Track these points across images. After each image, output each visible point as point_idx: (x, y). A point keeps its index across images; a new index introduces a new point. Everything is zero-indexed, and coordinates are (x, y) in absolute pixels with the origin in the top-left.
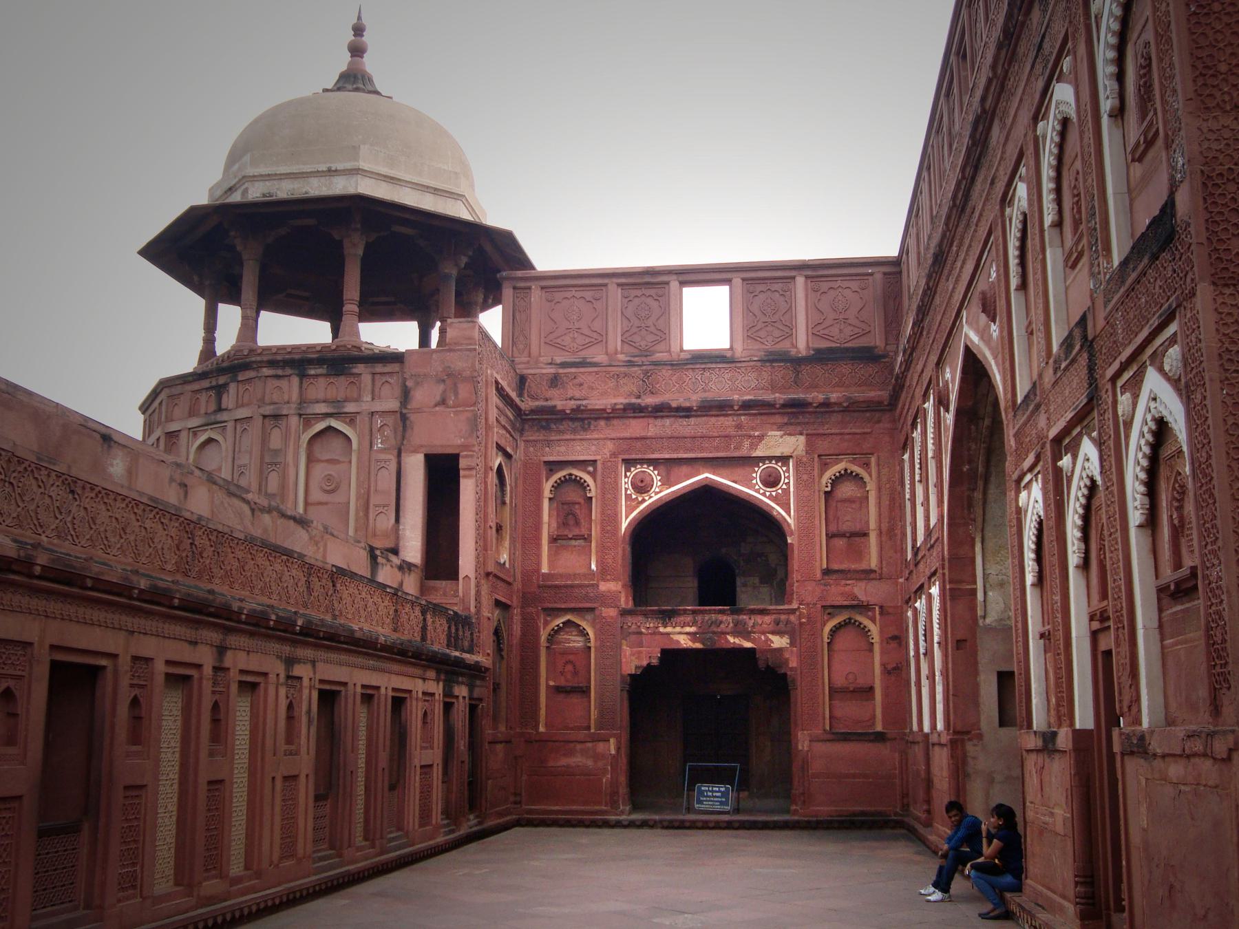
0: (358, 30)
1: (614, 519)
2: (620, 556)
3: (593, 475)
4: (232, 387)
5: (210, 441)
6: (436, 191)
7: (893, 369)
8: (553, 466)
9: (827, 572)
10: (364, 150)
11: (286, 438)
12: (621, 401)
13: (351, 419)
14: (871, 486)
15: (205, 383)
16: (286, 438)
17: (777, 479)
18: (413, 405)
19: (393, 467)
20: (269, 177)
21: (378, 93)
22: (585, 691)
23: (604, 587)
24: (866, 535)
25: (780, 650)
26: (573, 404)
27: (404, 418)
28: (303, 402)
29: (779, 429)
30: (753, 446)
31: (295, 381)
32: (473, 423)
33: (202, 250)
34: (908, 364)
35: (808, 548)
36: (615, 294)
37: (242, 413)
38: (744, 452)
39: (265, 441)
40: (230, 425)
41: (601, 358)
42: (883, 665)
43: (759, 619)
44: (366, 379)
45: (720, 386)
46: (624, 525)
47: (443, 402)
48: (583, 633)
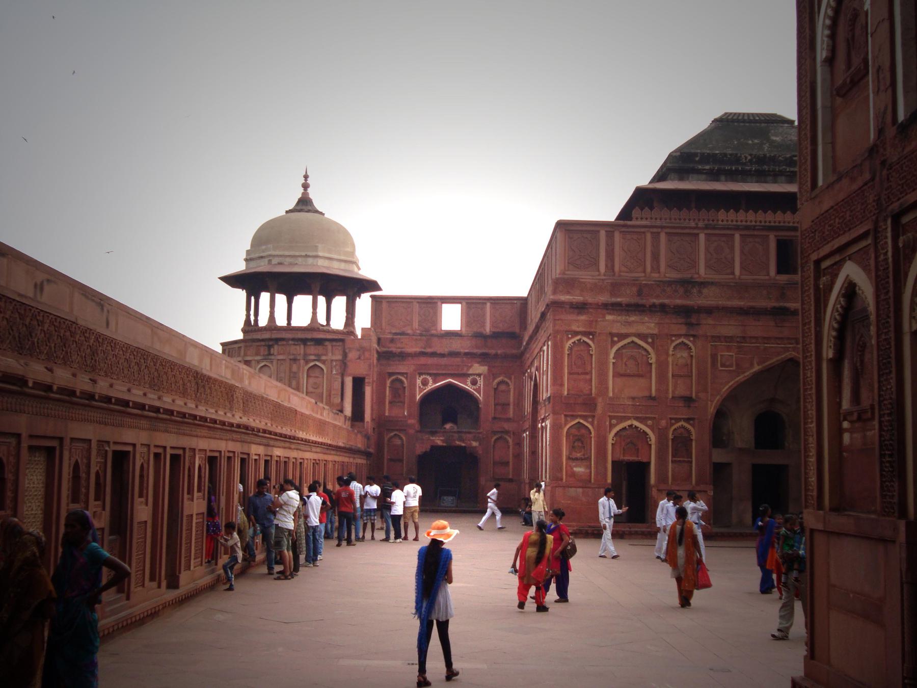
0: (306, 177)
1: (415, 396)
2: (416, 410)
3: (406, 378)
4: (276, 347)
5: (265, 365)
6: (345, 261)
7: (522, 343)
8: (391, 374)
9: (494, 418)
10: (320, 246)
11: (299, 368)
12: (418, 350)
13: (324, 362)
14: (512, 387)
15: (263, 343)
16: (299, 368)
17: (476, 382)
18: (348, 359)
19: (340, 380)
20: (281, 256)
21: (317, 211)
22: (401, 461)
23: (410, 421)
24: (509, 405)
25: (476, 447)
26: (399, 350)
27: (345, 364)
28: (305, 355)
29: (478, 363)
30: (468, 370)
31: (302, 346)
32: (370, 365)
33: (251, 282)
34: (526, 349)
35: (487, 409)
36: (416, 306)
37: (281, 357)
38: (464, 371)
39: (290, 369)
40: (275, 362)
41: (409, 332)
42: (513, 454)
43: (468, 435)
44: (330, 347)
45: (456, 345)
46: (418, 397)
47: (359, 358)
48: (401, 439)
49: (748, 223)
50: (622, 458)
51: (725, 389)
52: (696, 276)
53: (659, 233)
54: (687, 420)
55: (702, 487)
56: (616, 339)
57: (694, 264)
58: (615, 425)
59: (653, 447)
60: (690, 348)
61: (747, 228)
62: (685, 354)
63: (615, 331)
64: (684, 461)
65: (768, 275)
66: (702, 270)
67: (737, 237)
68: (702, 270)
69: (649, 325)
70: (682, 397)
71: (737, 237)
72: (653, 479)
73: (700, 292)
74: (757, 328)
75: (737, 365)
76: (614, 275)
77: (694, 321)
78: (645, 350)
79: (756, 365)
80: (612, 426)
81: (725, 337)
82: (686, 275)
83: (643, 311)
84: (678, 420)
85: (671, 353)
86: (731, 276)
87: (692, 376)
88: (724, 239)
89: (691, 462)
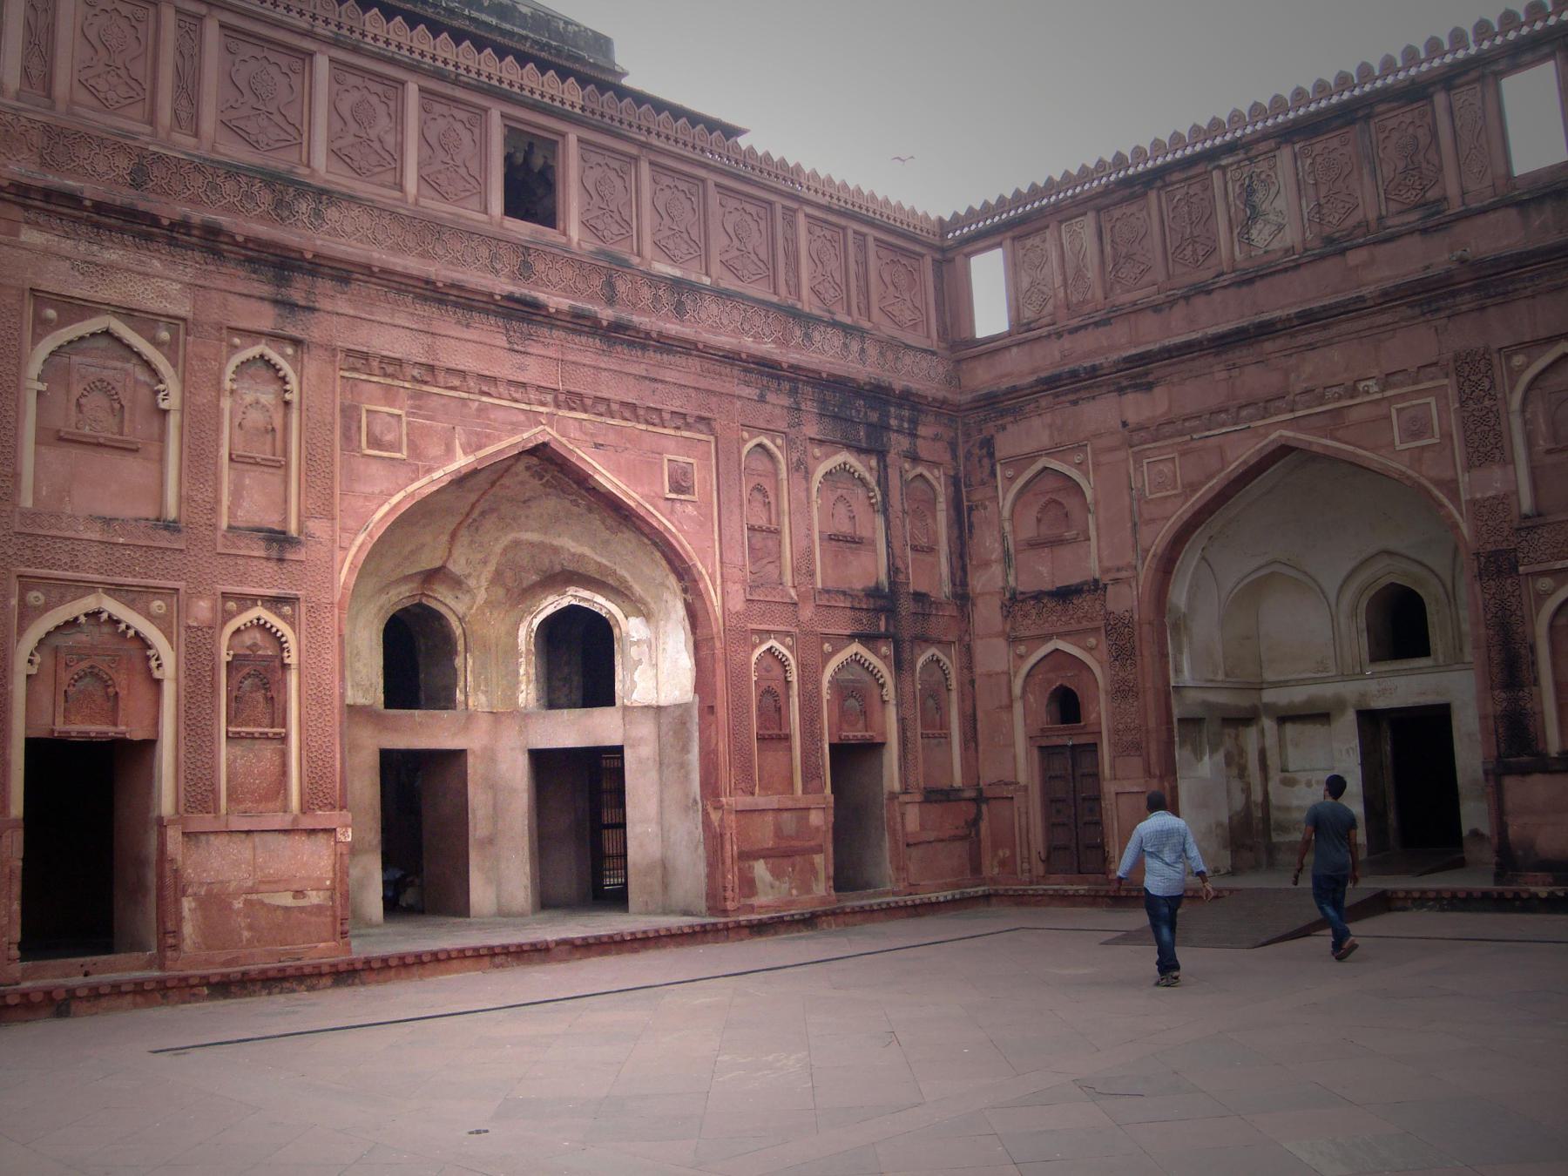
49: (439, 64)
50: (60, 727)
51: (381, 514)
52: (303, 171)
53: (200, 18)
54: (275, 602)
55: (322, 818)
56: (51, 313)
57: (297, 136)
58: (47, 608)
59: (169, 690)
60: (284, 380)
61: (439, 75)
62: (268, 396)
63: (49, 284)
64: (265, 737)
65: (486, 212)
66: (320, 159)
67: (412, 89)
68: (320, 159)
69: (164, 284)
70: (259, 530)
71: (412, 89)
72: (166, 800)
73: (318, 214)
74: (470, 346)
75: (413, 447)
76: (52, 107)
77: (298, 296)
78: (148, 365)
79: (459, 451)
80: (27, 614)
81: (384, 359)
82: (279, 161)
83: (149, 237)
84: (246, 601)
85: (227, 385)
86: (397, 194)
87: (286, 467)
88: (379, 88)
89: (284, 739)
